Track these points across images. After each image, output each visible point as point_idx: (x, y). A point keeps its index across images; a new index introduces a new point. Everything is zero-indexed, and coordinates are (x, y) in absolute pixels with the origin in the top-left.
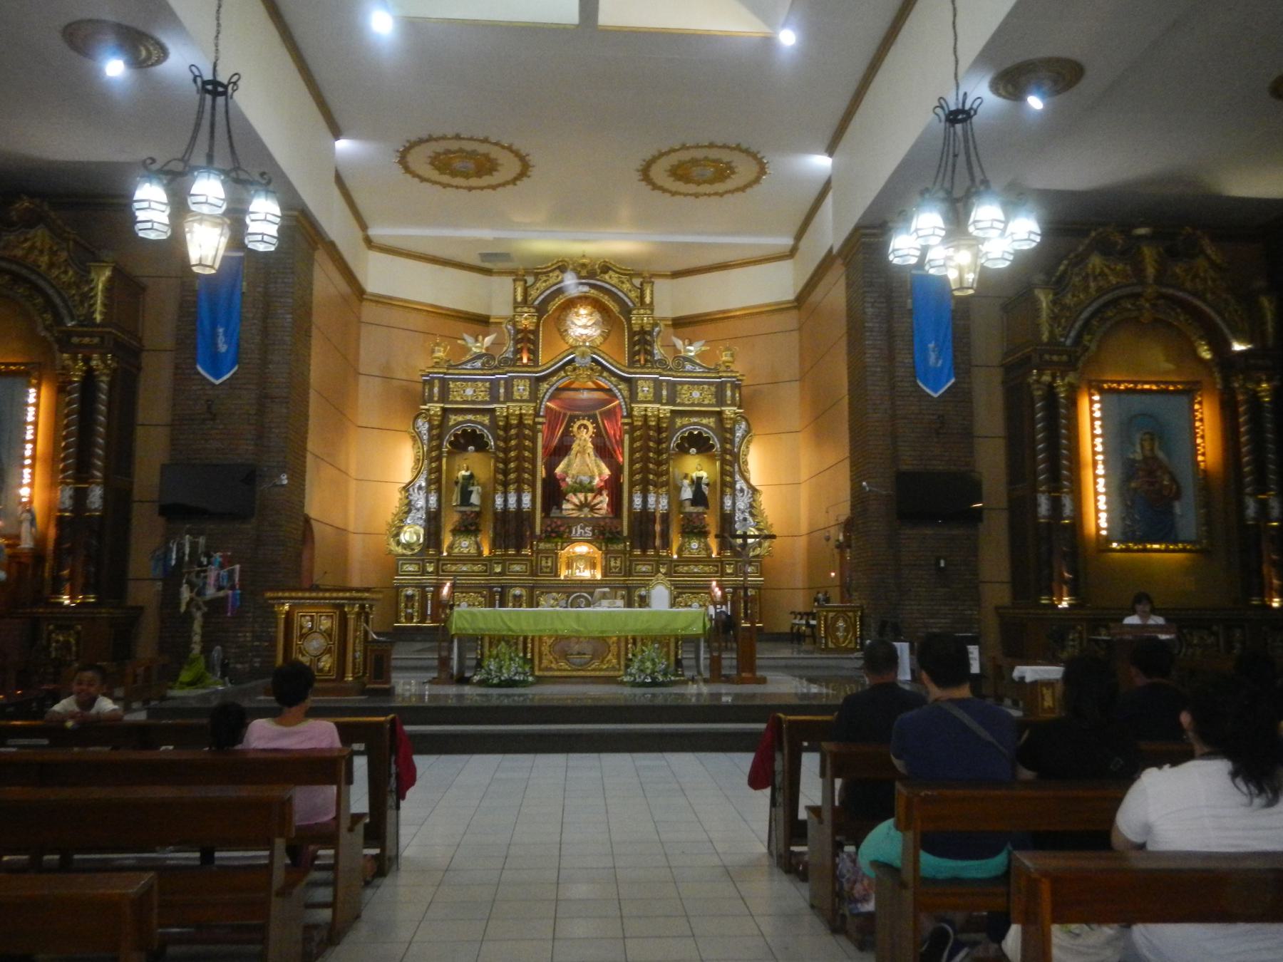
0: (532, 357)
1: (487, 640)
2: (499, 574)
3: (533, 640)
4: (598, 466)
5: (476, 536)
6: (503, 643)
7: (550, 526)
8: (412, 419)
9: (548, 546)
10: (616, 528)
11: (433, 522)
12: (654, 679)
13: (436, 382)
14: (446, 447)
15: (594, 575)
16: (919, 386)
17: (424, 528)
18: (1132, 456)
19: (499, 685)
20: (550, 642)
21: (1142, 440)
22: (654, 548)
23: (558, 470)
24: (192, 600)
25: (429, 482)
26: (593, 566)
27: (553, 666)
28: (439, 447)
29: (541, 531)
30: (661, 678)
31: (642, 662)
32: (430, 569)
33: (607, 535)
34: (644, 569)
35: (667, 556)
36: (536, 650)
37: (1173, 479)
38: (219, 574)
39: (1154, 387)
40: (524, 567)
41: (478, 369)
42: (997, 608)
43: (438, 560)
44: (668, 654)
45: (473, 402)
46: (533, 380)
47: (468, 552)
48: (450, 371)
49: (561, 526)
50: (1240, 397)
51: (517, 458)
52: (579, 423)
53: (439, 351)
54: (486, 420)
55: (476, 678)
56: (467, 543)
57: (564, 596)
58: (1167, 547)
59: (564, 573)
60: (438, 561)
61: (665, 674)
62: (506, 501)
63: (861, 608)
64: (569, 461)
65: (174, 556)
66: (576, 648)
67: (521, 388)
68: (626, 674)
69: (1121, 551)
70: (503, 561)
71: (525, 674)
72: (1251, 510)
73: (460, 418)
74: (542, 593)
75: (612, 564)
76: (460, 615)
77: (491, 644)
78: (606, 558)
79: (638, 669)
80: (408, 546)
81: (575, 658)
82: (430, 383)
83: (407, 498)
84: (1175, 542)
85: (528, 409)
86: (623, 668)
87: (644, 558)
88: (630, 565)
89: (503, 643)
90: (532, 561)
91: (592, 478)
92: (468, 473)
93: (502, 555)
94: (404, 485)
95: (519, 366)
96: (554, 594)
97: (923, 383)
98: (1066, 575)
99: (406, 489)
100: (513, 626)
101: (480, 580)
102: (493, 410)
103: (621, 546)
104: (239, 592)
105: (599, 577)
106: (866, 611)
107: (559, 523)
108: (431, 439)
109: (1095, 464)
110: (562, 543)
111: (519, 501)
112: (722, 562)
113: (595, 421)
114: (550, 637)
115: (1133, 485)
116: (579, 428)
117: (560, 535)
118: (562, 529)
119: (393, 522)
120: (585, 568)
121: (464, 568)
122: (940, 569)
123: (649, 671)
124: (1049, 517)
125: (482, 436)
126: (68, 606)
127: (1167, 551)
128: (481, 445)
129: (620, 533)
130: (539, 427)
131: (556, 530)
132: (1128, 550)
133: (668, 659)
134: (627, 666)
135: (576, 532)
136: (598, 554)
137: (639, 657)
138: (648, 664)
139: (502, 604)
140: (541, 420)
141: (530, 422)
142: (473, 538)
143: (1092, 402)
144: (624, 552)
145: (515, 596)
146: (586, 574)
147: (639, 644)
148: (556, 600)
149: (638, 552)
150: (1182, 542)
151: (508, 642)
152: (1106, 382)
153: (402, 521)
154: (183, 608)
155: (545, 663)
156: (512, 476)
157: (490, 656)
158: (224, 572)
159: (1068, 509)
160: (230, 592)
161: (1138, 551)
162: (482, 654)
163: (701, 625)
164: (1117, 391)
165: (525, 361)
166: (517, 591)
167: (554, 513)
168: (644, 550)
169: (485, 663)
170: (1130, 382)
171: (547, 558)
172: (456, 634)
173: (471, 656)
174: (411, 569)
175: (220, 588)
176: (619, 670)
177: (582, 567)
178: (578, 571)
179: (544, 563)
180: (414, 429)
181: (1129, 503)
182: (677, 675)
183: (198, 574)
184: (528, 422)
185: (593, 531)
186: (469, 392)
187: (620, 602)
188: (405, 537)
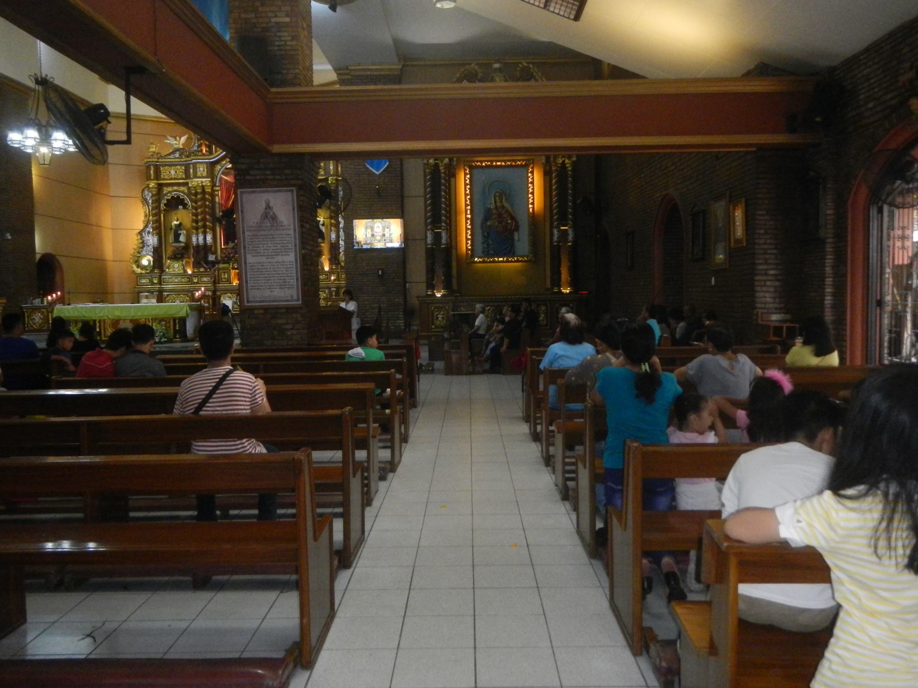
0: (207, 149)
2: (197, 283)
3: (100, 322)
5: (182, 261)
7: (225, 253)
8: (141, 191)
9: (225, 265)
11: (157, 253)
13: (152, 167)
14: (162, 206)
16: (368, 168)
17: (152, 257)
18: (489, 206)
21: (495, 196)
25: (154, 229)
28: (158, 207)
32: (155, 281)
37: (513, 218)
39: (503, 164)
40: (209, 278)
41: (178, 158)
42: (418, 297)
45: (175, 179)
48: (160, 160)
49: (230, 254)
50: (554, 168)
51: (202, 213)
53: (153, 148)
54: (184, 189)
56: (177, 265)
57: (235, 295)
58: (507, 259)
62: (198, 239)
67: (201, 169)
69: (480, 262)
72: (555, 238)
73: (170, 189)
74: (222, 294)
80: (144, 268)
82: (148, 168)
83: (141, 239)
84: (513, 256)
85: (206, 181)
92: (178, 223)
94: (139, 231)
95: (201, 156)
97: (372, 166)
99: (140, 233)
100: (86, 315)
101: (187, 287)
102: (187, 184)
108: (152, 203)
109: (466, 210)
111: (205, 239)
115: (488, 223)
119: (134, 253)
122: (379, 276)
124: (433, 244)
125: (183, 200)
127: (507, 261)
128: (185, 206)
130: (216, 193)
132: (484, 262)
140: (217, 188)
141: (210, 190)
143: (466, 174)
150: (517, 257)
152: (474, 162)
153: (139, 253)
156: (200, 224)
159: (444, 241)
161: (490, 262)
163: (185, 312)
164: (482, 167)
165: (204, 152)
170: (488, 161)
171: (224, 273)
179: (223, 276)
180: (142, 196)
181: (485, 234)
184: (208, 190)
186: (173, 172)
187: (154, 301)
188: (145, 262)
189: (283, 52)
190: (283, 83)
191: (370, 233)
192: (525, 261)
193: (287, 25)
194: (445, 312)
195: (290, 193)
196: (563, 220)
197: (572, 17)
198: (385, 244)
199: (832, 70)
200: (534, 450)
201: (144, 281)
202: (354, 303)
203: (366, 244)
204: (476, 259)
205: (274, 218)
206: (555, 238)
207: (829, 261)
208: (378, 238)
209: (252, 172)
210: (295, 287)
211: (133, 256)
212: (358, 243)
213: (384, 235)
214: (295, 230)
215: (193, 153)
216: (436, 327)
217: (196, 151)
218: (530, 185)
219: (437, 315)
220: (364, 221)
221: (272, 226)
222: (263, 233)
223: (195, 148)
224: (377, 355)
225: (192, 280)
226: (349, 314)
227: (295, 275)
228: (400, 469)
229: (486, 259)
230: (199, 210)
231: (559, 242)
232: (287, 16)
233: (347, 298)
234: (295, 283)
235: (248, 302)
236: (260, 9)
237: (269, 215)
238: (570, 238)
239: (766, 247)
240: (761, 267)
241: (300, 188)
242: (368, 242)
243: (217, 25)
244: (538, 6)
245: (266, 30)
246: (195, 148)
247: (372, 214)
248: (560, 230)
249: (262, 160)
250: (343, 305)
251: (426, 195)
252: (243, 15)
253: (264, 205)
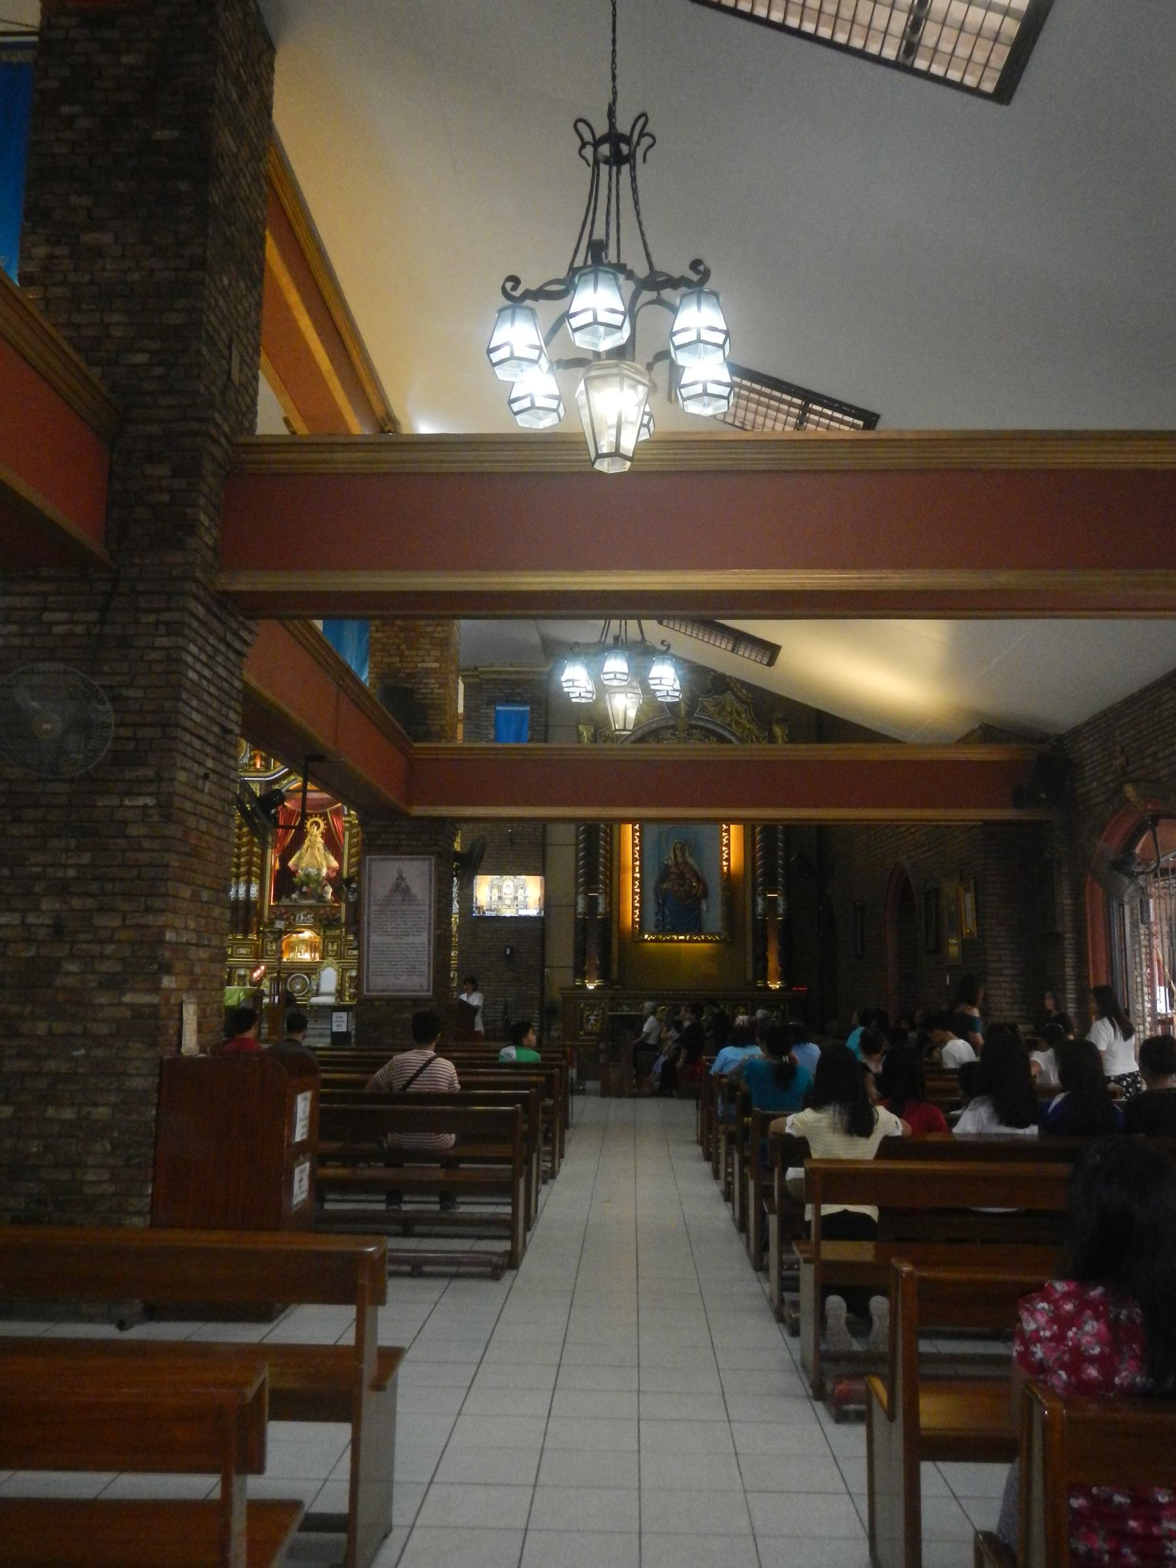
4: (326, 859)
10: (334, 915)
23: (291, 864)
33: (324, 922)
37: (700, 880)
46: (263, 786)
52: (311, 820)
64: (300, 855)
69: (652, 941)
72: (760, 909)
75: (330, 948)
78: (324, 943)
84: (699, 933)
91: (319, 870)
103: (338, 932)
107: (284, 911)
111: (248, 891)
113: (326, 819)
115: (665, 886)
116: (312, 824)
120: (306, 951)
122: (509, 957)
124: (585, 914)
127: (691, 941)
129: (340, 919)
132: (657, 941)
136: (318, 940)
145: (240, 976)
150: (705, 935)
159: (601, 909)
161: (666, 941)
165: (258, 766)
167: (285, 901)
179: (269, 947)
189: (429, 702)
190: (427, 736)
191: (497, 895)
192: (717, 941)
193: (434, 670)
194: (600, 1012)
195: (427, 862)
196: (770, 885)
197: (765, 662)
198: (517, 911)
199: (1060, 738)
200: (707, 1167)
202: (479, 994)
203: (490, 910)
204: (646, 936)
205: (407, 890)
206: (760, 909)
207: (1070, 960)
208: (508, 902)
209: (383, 837)
210: (426, 974)
212: (478, 908)
213: (516, 898)
214: (430, 906)
215: (242, 767)
216: (587, 1034)
217: (245, 764)
218: (724, 834)
219: (588, 1015)
220: (489, 878)
221: (404, 900)
222: (392, 908)
223: (246, 761)
224: (531, 1056)
226: (474, 1010)
227: (426, 959)
228: (559, 1177)
229: (661, 937)
230: (243, 850)
231: (764, 915)
232: (436, 661)
233: (470, 987)
234: (426, 970)
235: (368, 990)
236: (406, 653)
237: (401, 888)
238: (781, 910)
239: (1000, 940)
240: (993, 965)
241: (440, 856)
242: (493, 907)
243: (351, 659)
244: (725, 649)
245: (411, 676)
246: (246, 761)
247: (501, 869)
248: (765, 899)
249: (397, 823)
250: (464, 997)
251: (577, 844)
252: (387, 660)
253: (396, 876)
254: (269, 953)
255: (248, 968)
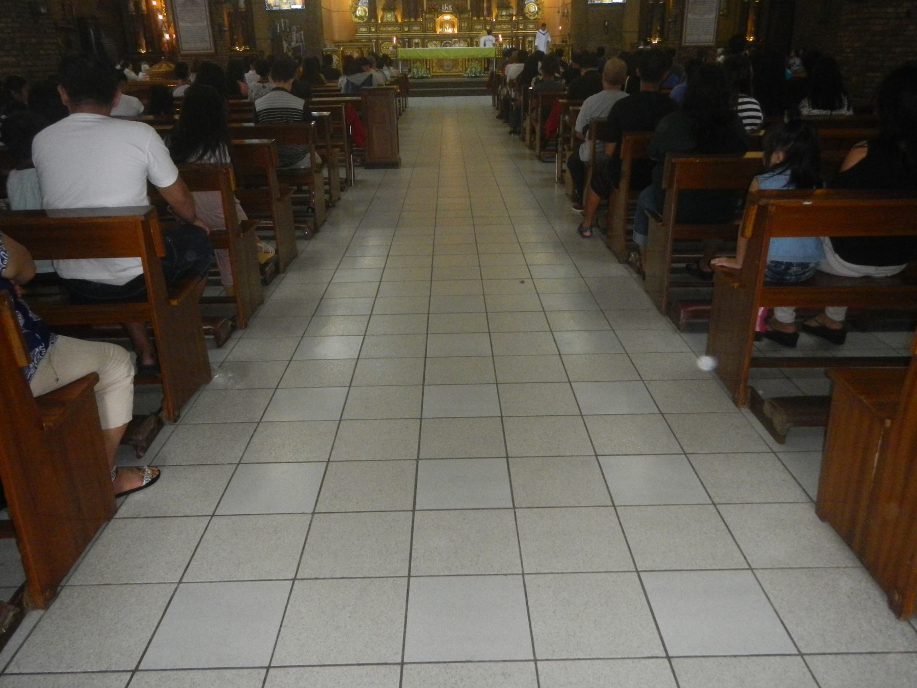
1: (412, 61)
6: (418, 62)
7: (431, 5)
9: (430, 16)
10: (464, 5)
12: (475, 73)
15: (454, 31)
19: (418, 78)
20: (436, 61)
22: (483, 15)
24: (287, 47)
26: (453, 26)
27: (438, 71)
29: (427, 9)
30: (478, 75)
31: (471, 68)
32: (373, 30)
34: (478, 28)
35: (490, 20)
36: (431, 65)
38: (296, 36)
40: (419, 27)
43: (377, 25)
44: (481, 65)
47: (391, 20)
55: (409, 76)
59: (439, 30)
60: (377, 25)
61: (480, 73)
63: (572, 45)
65: (278, 28)
66: (446, 64)
68: (466, 73)
70: (409, 25)
71: (427, 74)
75: (463, 25)
76: (401, 51)
77: (413, 63)
79: (470, 71)
80: (361, 17)
81: (446, 68)
86: (464, 71)
87: (479, 22)
88: (472, 26)
89: (418, 62)
90: (422, 24)
93: (406, 22)
96: (435, 42)
98: (658, 28)
104: (304, 43)
105: (456, 32)
106: (574, 47)
110: (437, 15)
112: (517, 23)
114: (436, 59)
117: (436, 10)
118: (437, 7)
119: (352, 4)
121: (390, 29)
123: (473, 72)
126: (239, 52)
129: (467, 8)
131: (434, 7)
133: (481, 68)
134: (466, 70)
135: (444, 7)
136: (456, 20)
137: (470, 67)
138: (474, 69)
139: (409, 47)
142: (393, 13)
144: (468, 18)
146: (450, 31)
147: (470, 62)
148: (435, 44)
149: (475, 18)
151: (420, 61)
153: (357, 5)
154: (285, 51)
155: (434, 70)
157: (414, 67)
158: (298, 35)
160: (301, 44)
162: (410, 67)
166: (416, 41)
168: (478, 17)
169: (412, 70)
172: (400, 59)
173: (406, 70)
174: (364, 30)
175: (297, 42)
176: (463, 72)
177: (448, 27)
178: (445, 29)
182: (485, 73)
183: (287, 36)
185: (452, 7)
188: (358, 13)
201: (364, 30)
211: (352, 7)
225: (403, 29)
254: (429, 29)
255: (420, 38)
